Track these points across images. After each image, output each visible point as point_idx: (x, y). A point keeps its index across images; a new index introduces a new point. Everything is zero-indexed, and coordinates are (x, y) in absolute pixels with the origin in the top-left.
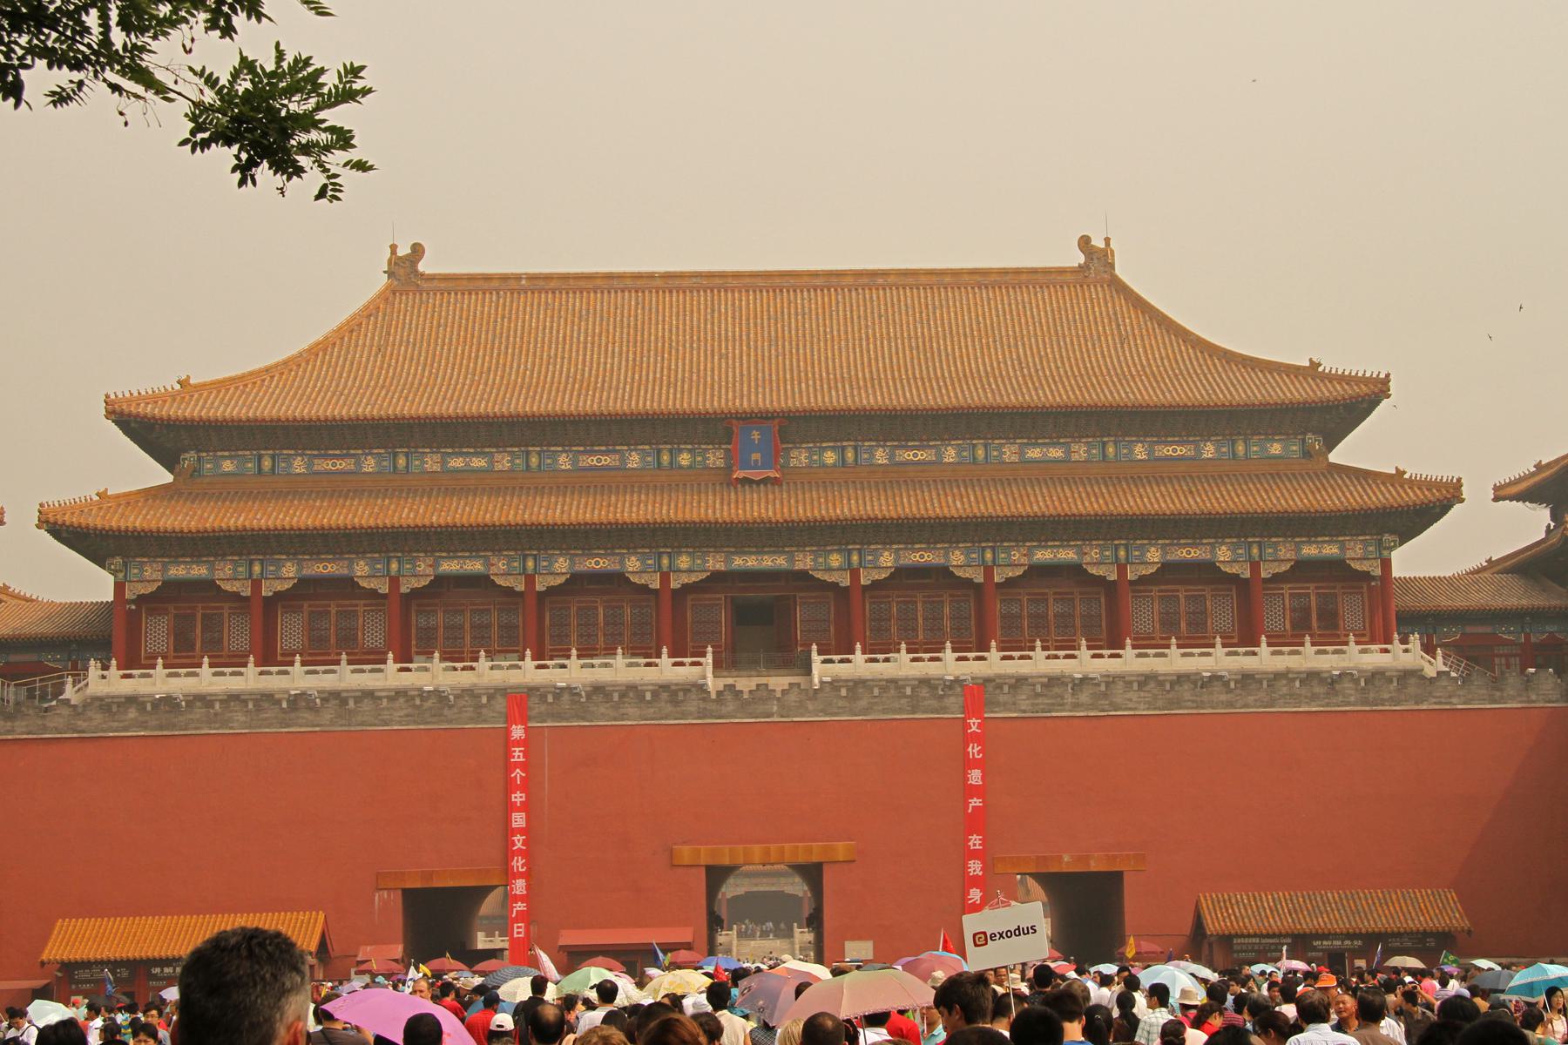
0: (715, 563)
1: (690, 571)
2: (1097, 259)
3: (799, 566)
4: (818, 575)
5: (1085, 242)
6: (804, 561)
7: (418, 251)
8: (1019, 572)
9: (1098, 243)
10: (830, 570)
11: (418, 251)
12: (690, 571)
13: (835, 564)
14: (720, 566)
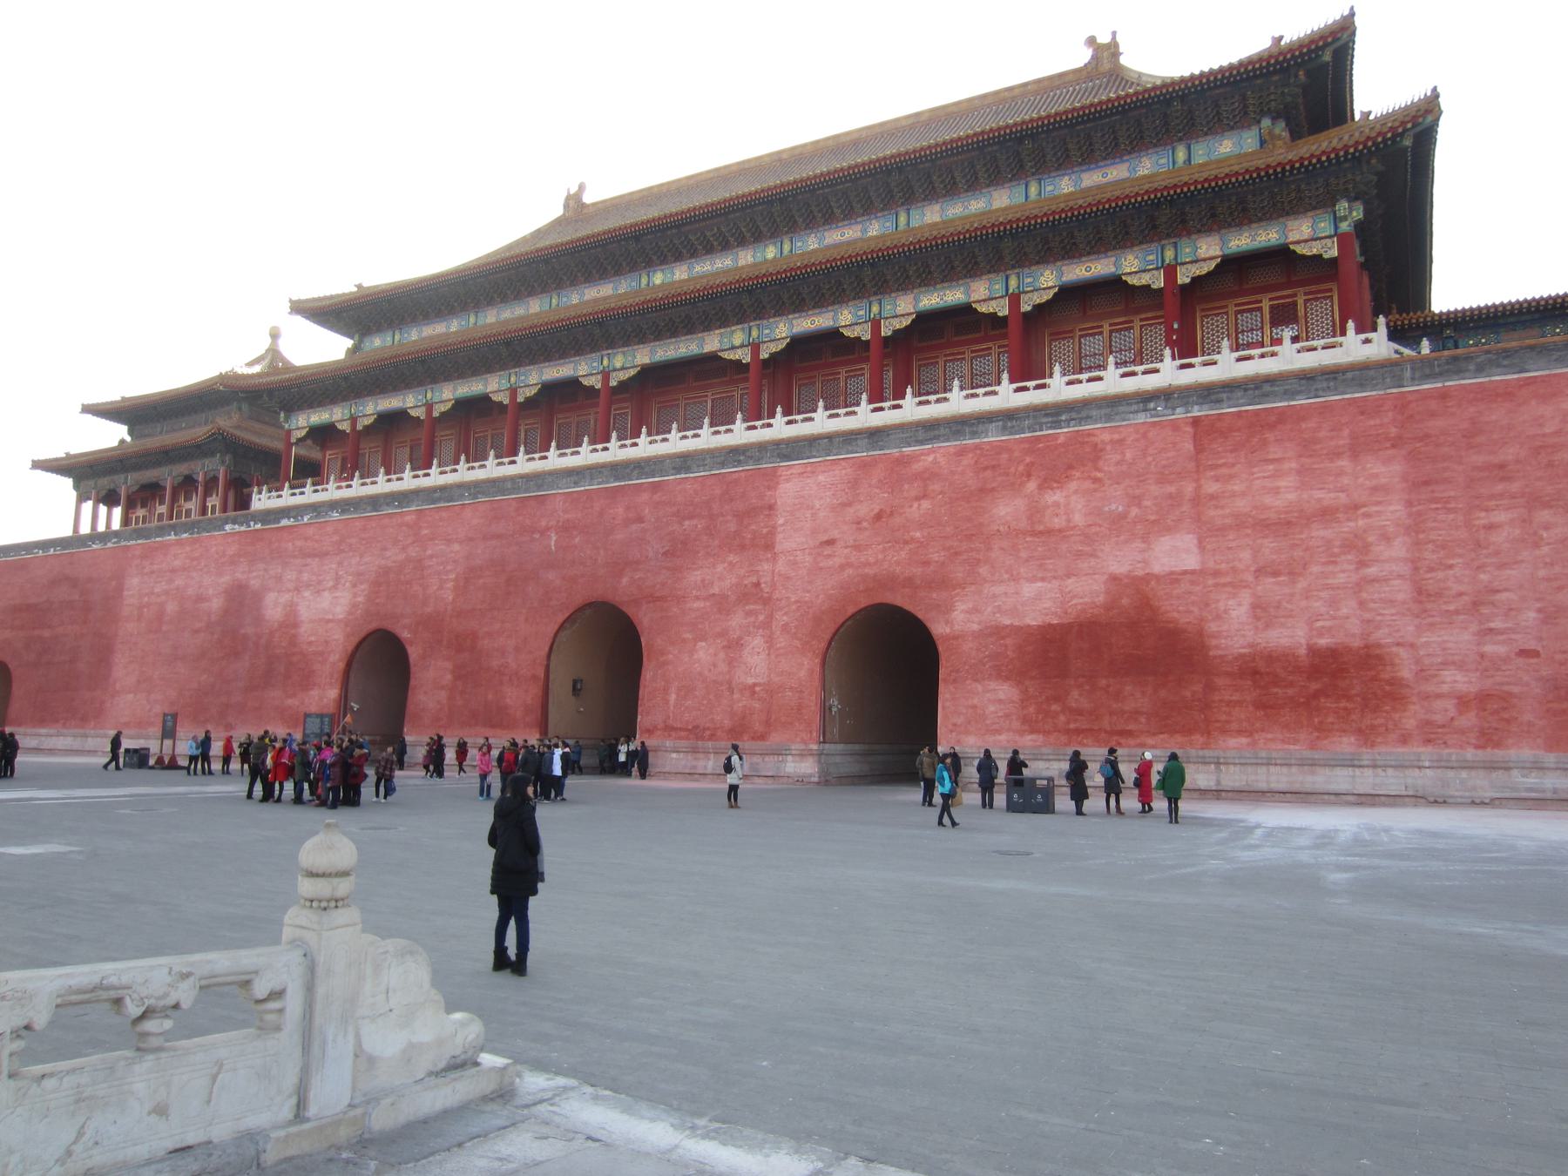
0: (644, 355)
1: (623, 368)
2: (1106, 53)
3: (707, 349)
4: (725, 355)
5: (1091, 41)
6: (711, 342)
7: (582, 187)
8: (906, 322)
9: (1104, 39)
10: (733, 348)
11: (582, 187)
12: (623, 368)
13: (737, 342)
14: (646, 360)
